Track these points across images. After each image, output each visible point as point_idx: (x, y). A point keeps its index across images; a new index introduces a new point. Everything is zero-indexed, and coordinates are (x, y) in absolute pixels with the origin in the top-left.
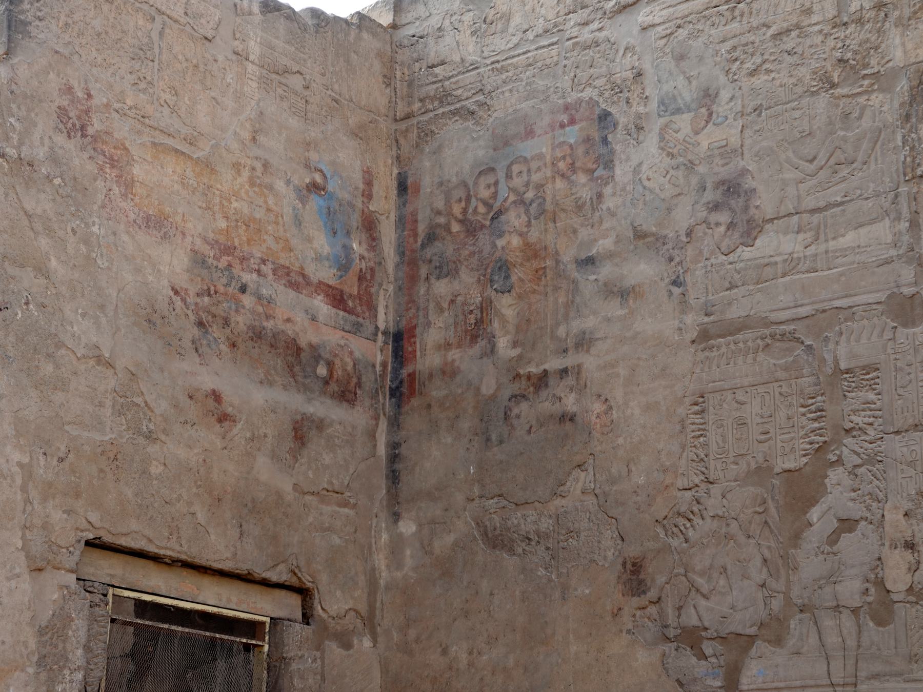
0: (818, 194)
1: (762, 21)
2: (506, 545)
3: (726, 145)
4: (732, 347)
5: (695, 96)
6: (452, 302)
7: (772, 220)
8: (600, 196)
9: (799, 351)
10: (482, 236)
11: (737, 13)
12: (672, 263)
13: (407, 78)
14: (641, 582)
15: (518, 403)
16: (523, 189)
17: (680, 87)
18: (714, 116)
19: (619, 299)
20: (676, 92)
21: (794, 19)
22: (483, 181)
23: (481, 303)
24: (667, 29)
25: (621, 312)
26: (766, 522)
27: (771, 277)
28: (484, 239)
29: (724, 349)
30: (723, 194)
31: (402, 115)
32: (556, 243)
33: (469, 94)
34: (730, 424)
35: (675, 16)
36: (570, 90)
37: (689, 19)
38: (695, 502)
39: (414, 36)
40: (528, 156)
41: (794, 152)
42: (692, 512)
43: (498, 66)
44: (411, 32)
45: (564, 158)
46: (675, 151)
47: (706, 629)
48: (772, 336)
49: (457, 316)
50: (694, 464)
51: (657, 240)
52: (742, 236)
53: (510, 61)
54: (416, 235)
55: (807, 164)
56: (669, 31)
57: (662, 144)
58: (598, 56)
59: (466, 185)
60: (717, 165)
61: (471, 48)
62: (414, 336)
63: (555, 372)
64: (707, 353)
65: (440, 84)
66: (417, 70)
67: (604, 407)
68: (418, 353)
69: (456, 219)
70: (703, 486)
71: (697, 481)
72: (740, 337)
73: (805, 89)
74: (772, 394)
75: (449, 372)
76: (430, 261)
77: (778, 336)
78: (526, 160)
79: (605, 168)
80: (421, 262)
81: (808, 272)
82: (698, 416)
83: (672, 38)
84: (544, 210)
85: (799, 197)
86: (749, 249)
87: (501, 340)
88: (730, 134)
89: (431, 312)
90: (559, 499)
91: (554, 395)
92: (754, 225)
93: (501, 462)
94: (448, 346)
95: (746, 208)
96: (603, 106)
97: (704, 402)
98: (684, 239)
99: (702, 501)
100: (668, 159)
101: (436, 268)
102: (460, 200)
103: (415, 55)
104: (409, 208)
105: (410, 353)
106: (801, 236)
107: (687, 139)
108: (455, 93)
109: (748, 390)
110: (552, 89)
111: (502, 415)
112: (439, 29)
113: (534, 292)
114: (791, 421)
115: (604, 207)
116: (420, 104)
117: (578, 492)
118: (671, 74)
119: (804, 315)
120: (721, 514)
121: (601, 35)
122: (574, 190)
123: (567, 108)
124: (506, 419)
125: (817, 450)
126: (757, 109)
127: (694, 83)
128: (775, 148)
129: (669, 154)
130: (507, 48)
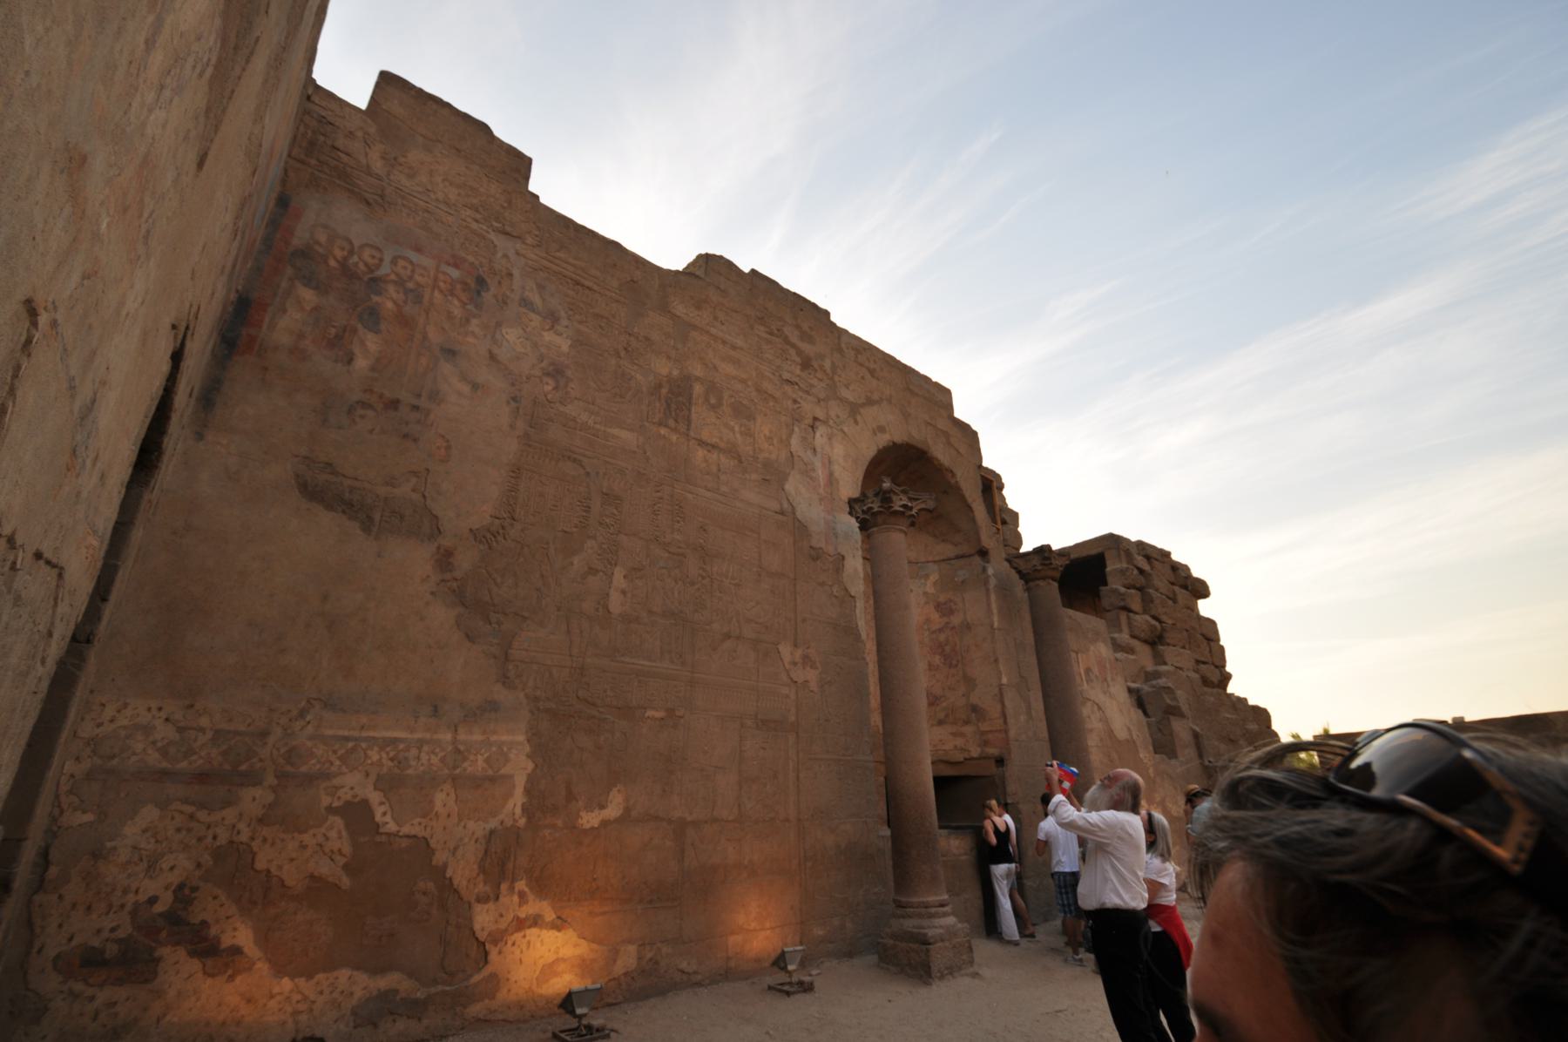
8: (468, 321)
59: (351, 243)
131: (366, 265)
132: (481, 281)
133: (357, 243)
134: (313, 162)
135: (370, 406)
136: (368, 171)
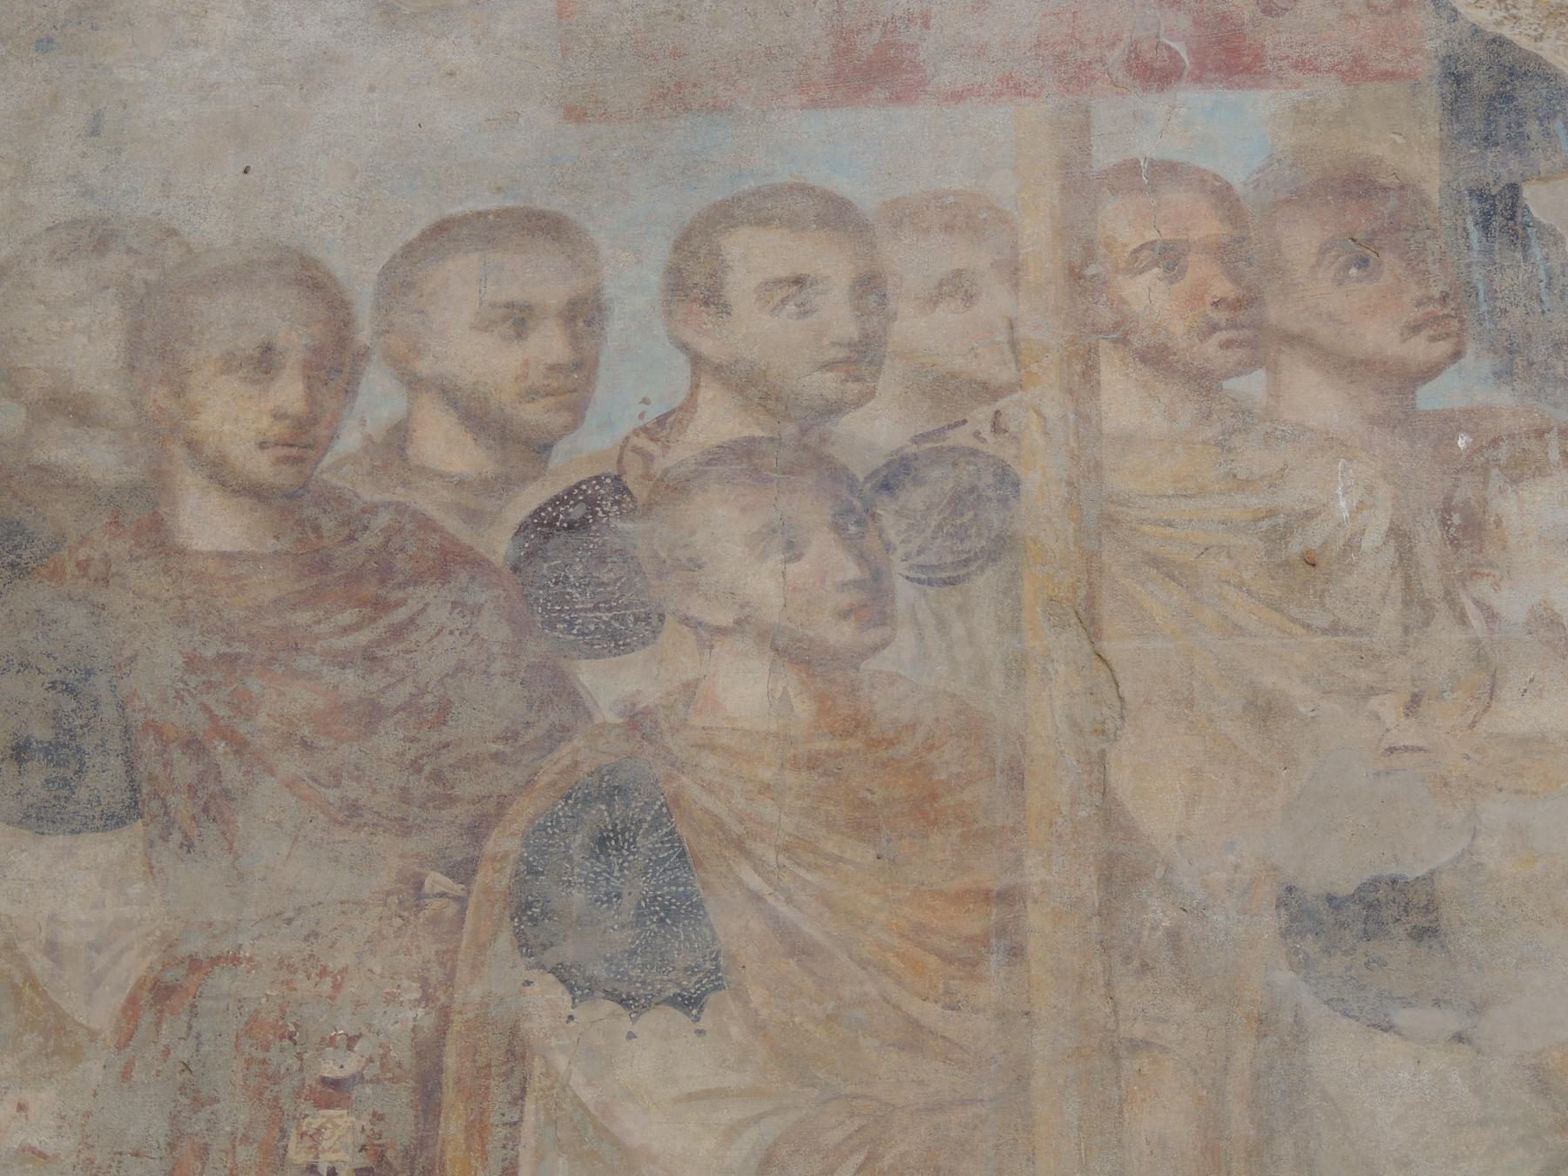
6: (161, 993)
8: (1468, 530)
22: (461, 287)
23: (429, 1052)
40: (863, 193)
59: (313, 281)
69: (222, 475)
78: (836, 215)
79: (1504, 375)
84: (1002, 546)
102: (265, 362)
113: (914, 1037)
115: (1513, 603)
131: (476, 416)
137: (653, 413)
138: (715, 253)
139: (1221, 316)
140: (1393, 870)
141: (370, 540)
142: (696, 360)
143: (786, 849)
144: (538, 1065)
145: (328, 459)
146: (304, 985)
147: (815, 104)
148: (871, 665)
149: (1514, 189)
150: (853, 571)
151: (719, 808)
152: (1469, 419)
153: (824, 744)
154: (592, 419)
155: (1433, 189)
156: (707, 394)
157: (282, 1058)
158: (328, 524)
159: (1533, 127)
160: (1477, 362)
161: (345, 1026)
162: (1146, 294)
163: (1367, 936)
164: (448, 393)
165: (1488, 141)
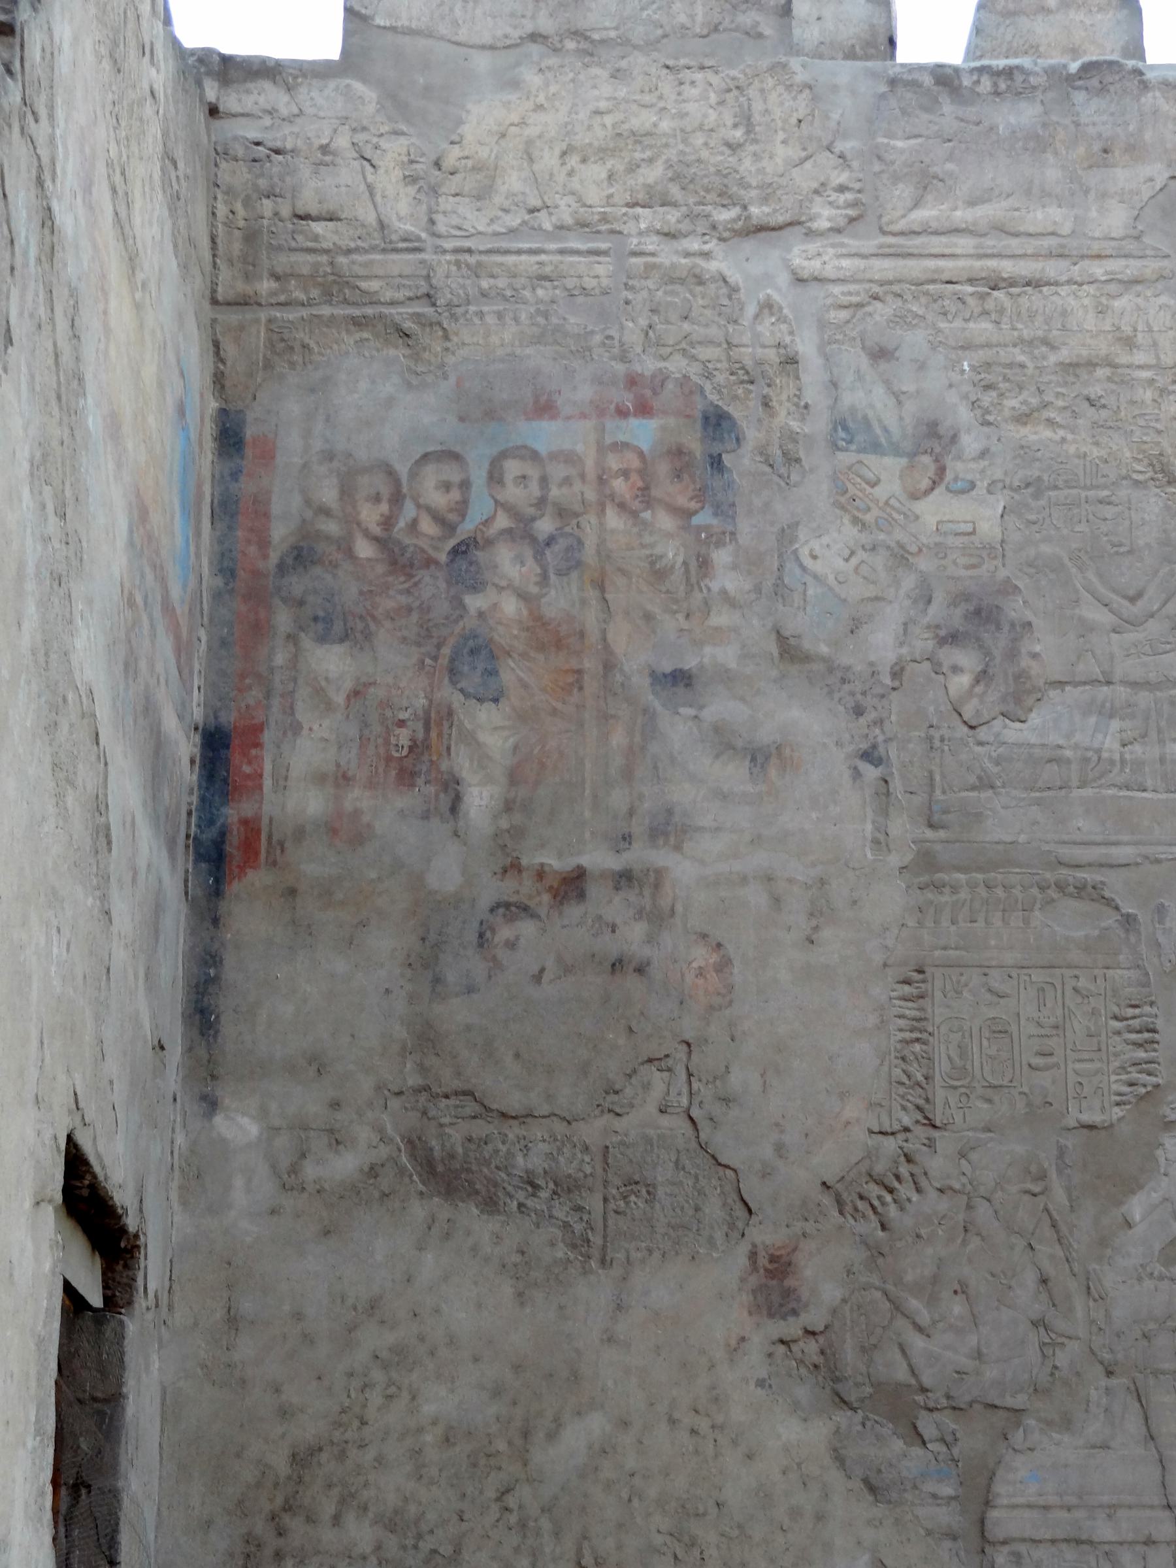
0: (1145, 659)
1: (1040, 333)
2: (477, 1192)
3: (973, 533)
4: (983, 892)
5: (910, 430)
6: (356, 693)
7: (1061, 684)
8: (705, 564)
9: (1110, 920)
10: (427, 579)
11: (990, 305)
12: (862, 720)
13: (241, 224)
14: (788, 1293)
15: (510, 919)
16: (531, 511)
17: (879, 406)
18: (949, 475)
19: (747, 763)
20: (871, 414)
21: (1103, 347)
22: (431, 476)
23: (427, 713)
24: (850, 294)
25: (750, 788)
26: (1046, 1210)
27: (1058, 784)
28: (432, 585)
29: (964, 895)
30: (966, 617)
31: (231, 296)
32: (604, 632)
33: (400, 295)
34: (975, 1031)
35: (868, 276)
36: (639, 350)
37: (896, 288)
38: (902, 1159)
39: (258, 144)
40: (542, 448)
41: (1100, 576)
42: (898, 1177)
43: (472, 260)
44: (253, 135)
45: (625, 473)
46: (869, 518)
47: (924, 1390)
48: (1060, 887)
49: (365, 724)
50: (902, 1090)
51: (831, 670)
52: (1004, 699)
53: (499, 259)
54: (264, 544)
55: (1126, 603)
56: (855, 299)
57: (843, 500)
58: (701, 302)
59: (391, 473)
60: (955, 563)
61: (403, 207)
62: (258, 745)
63: (603, 875)
64: (930, 896)
65: (324, 259)
66: (268, 213)
67: (714, 958)
68: (267, 783)
69: (367, 534)
70: (921, 1132)
71: (907, 1121)
72: (996, 876)
73: (1124, 472)
74: (1059, 987)
75: (344, 831)
76: (301, 603)
77: (1071, 889)
78: (535, 456)
79: (716, 514)
80: (277, 601)
81: (1128, 788)
82: (910, 1004)
83: (860, 314)
84: (579, 564)
85: (1112, 657)
86: (1018, 725)
87: (475, 791)
88: (984, 515)
89: (300, 706)
90: (608, 1117)
91: (600, 917)
92: (1028, 686)
93: (469, 1028)
94: (343, 779)
95: (1012, 654)
96: (713, 397)
97: (923, 981)
98: (888, 681)
99: (917, 1158)
100: (855, 531)
101: (316, 619)
102: (377, 499)
103: (263, 183)
104: (246, 487)
105: (248, 776)
106: (1115, 724)
107: (892, 502)
108: (364, 285)
109: (1014, 974)
110: (598, 338)
111: (472, 936)
112: (324, 149)
113: (554, 712)
114: (1095, 1040)
115: (715, 586)
116: (274, 285)
117: (651, 1108)
118: (859, 376)
119: (1125, 862)
120: (957, 1186)
121: (713, 266)
122: (647, 539)
123: (632, 381)
124: (481, 945)
125: (1141, 1098)
126: (1035, 486)
127: (910, 407)
128: (1066, 561)
129: (855, 521)
130: (490, 230)
132: (717, 423)
133: (403, 470)
134: (266, 286)
135: (525, 910)
136: (387, 240)
137: (485, 518)
138: (501, 467)
139: (639, 493)
140: (680, 666)
141: (408, 555)
142: (496, 501)
143: (519, 655)
144: (456, 718)
145: (395, 530)
146: (394, 692)
147: (528, 419)
148: (543, 600)
149: (720, 455)
150: (539, 571)
151: (503, 643)
152: (706, 528)
153: (531, 624)
154: (468, 519)
155: (698, 454)
156: (500, 512)
157: (389, 713)
158: (396, 550)
159: (726, 435)
160: (708, 510)
161: (405, 703)
162: (619, 485)
163: (673, 685)
164: (428, 509)
165: (714, 439)
